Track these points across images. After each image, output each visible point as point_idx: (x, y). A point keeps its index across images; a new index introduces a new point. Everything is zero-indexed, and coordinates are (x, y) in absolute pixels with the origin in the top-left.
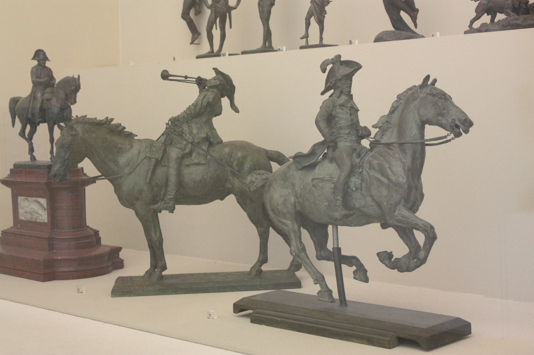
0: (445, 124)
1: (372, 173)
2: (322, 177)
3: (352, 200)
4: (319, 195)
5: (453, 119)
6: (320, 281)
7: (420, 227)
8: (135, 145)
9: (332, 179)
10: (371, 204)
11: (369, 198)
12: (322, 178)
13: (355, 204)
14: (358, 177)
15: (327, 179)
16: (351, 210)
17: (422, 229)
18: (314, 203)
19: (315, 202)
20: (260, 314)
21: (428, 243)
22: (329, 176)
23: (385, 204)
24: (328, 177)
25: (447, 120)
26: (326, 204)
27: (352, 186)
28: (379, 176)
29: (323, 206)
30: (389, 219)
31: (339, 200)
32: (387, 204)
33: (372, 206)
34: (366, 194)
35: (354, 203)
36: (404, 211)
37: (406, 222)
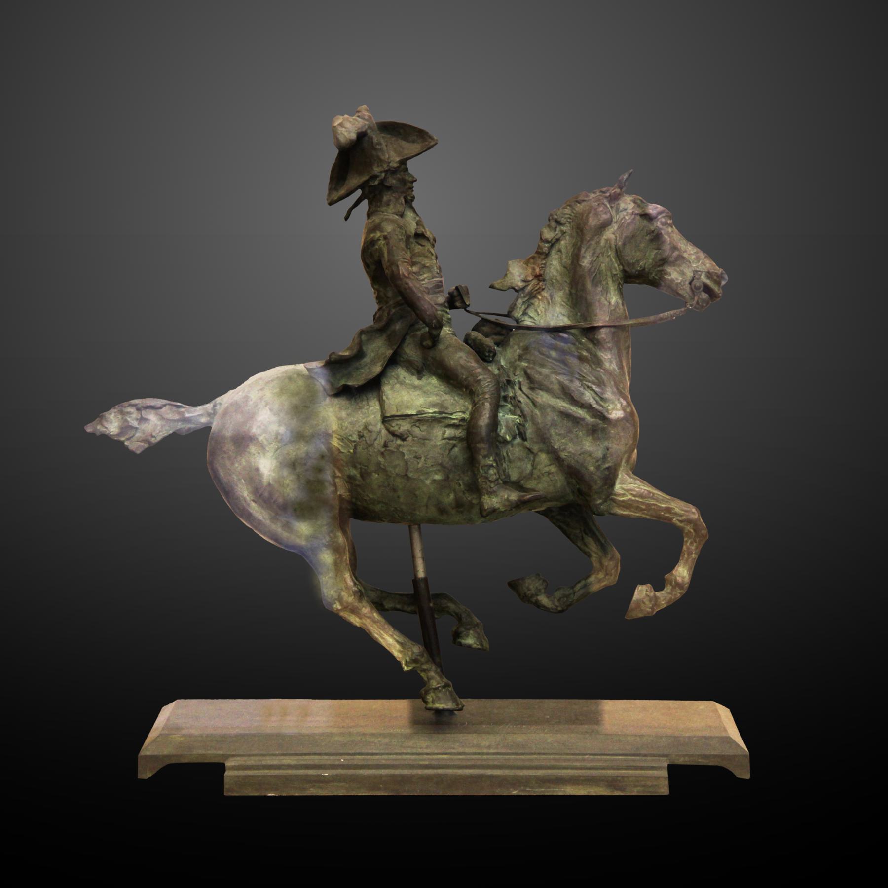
0: (679, 281)
1: (543, 397)
2: (414, 413)
3: (502, 464)
4: (416, 457)
5: (695, 272)
6: (422, 664)
7: (676, 514)
8: (516, 357)
9: (444, 415)
10: (547, 469)
11: (543, 457)
12: (417, 415)
13: (508, 472)
14: (512, 408)
15: (432, 417)
16: (524, 492)
17: (680, 519)
18: (406, 476)
19: (406, 475)
20: (618, 769)
21: (693, 548)
22: (436, 410)
23: (592, 468)
24: (435, 413)
25: (683, 274)
26: (438, 477)
27: (503, 431)
28: (562, 404)
29: (428, 482)
30: (599, 502)
31: (492, 466)
32: (598, 468)
33: (549, 473)
34: (535, 448)
35: (507, 471)
36: (629, 480)
37: (643, 507)
